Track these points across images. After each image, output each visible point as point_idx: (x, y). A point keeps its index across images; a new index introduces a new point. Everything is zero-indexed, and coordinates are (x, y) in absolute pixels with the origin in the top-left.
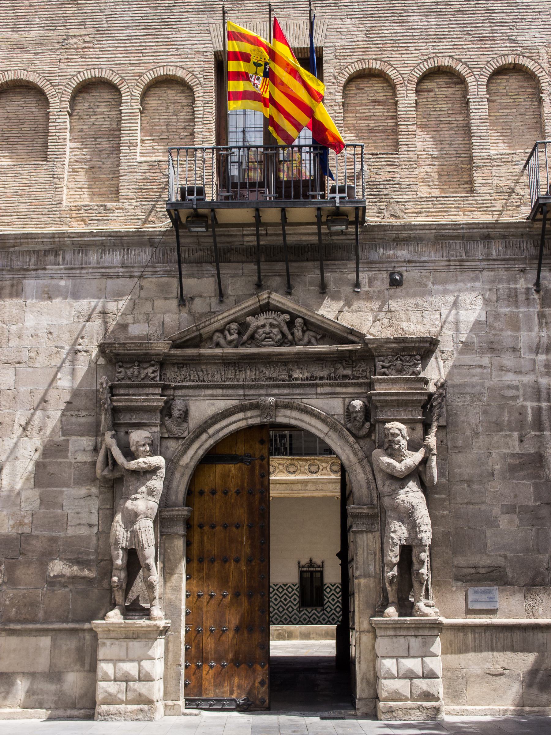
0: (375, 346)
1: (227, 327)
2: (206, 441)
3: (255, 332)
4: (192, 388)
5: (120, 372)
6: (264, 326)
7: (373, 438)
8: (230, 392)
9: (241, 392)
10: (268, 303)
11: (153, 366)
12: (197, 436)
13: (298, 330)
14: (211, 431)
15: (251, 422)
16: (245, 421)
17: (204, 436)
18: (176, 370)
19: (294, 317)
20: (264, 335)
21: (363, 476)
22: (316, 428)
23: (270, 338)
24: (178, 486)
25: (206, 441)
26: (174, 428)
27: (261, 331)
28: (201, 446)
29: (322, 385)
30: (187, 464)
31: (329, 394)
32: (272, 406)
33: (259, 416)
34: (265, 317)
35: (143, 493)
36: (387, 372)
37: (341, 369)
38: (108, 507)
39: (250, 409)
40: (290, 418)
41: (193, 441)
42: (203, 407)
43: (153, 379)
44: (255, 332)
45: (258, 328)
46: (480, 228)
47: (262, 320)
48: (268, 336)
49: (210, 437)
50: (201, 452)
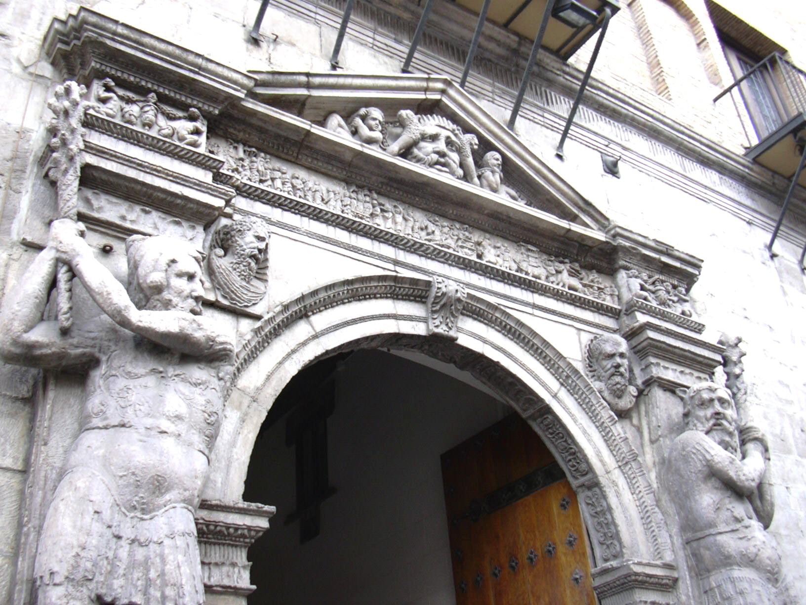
0: (627, 244)
1: (363, 111)
2: (304, 344)
3: (415, 144)
4: (280, 206)
5: (104, 101)
6: (434, 138)
7: (635, 421)
8: (364, 243)
9: (388, 251)
10: (439, 101)
11: (192, 118)
12: (288, 323)
13: (493, 172)
14: (321, 320)
15: (407, 328)
16: (392, 322)
17: (302, 330)
18: (241, 154)
19: (485, 146)
20: (435, 157)
21: (631, 497)
22: (536, 377)
23: (444, 165)
24: (233, 444)
25: (304, 344)
26: (236, 281)
27: (428, 147)
28: (294, 351)
29: (543, 291)
30: (259, 390)
31: (554, 312)
32: (459, 300)
33: (425, 320)
34: (437, 122)
35: (179, 417)
36: (650, 298)
37: (565, 274)
38: (8, 462)
39: (406, 298)
40: (485, 341)
41: (276, 332)
42: (301, 260)
43: (194, 144)
44: (415, 144)
45: (424, 137)
46: (702, 143)
47: (432, 124)
48: (442, 160)
49: (316, 337)
50: (292, 369)
